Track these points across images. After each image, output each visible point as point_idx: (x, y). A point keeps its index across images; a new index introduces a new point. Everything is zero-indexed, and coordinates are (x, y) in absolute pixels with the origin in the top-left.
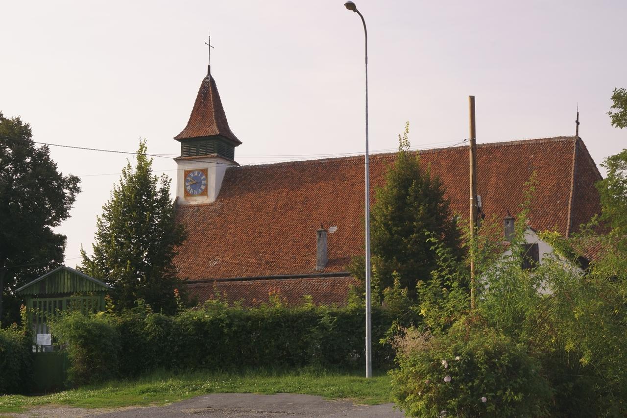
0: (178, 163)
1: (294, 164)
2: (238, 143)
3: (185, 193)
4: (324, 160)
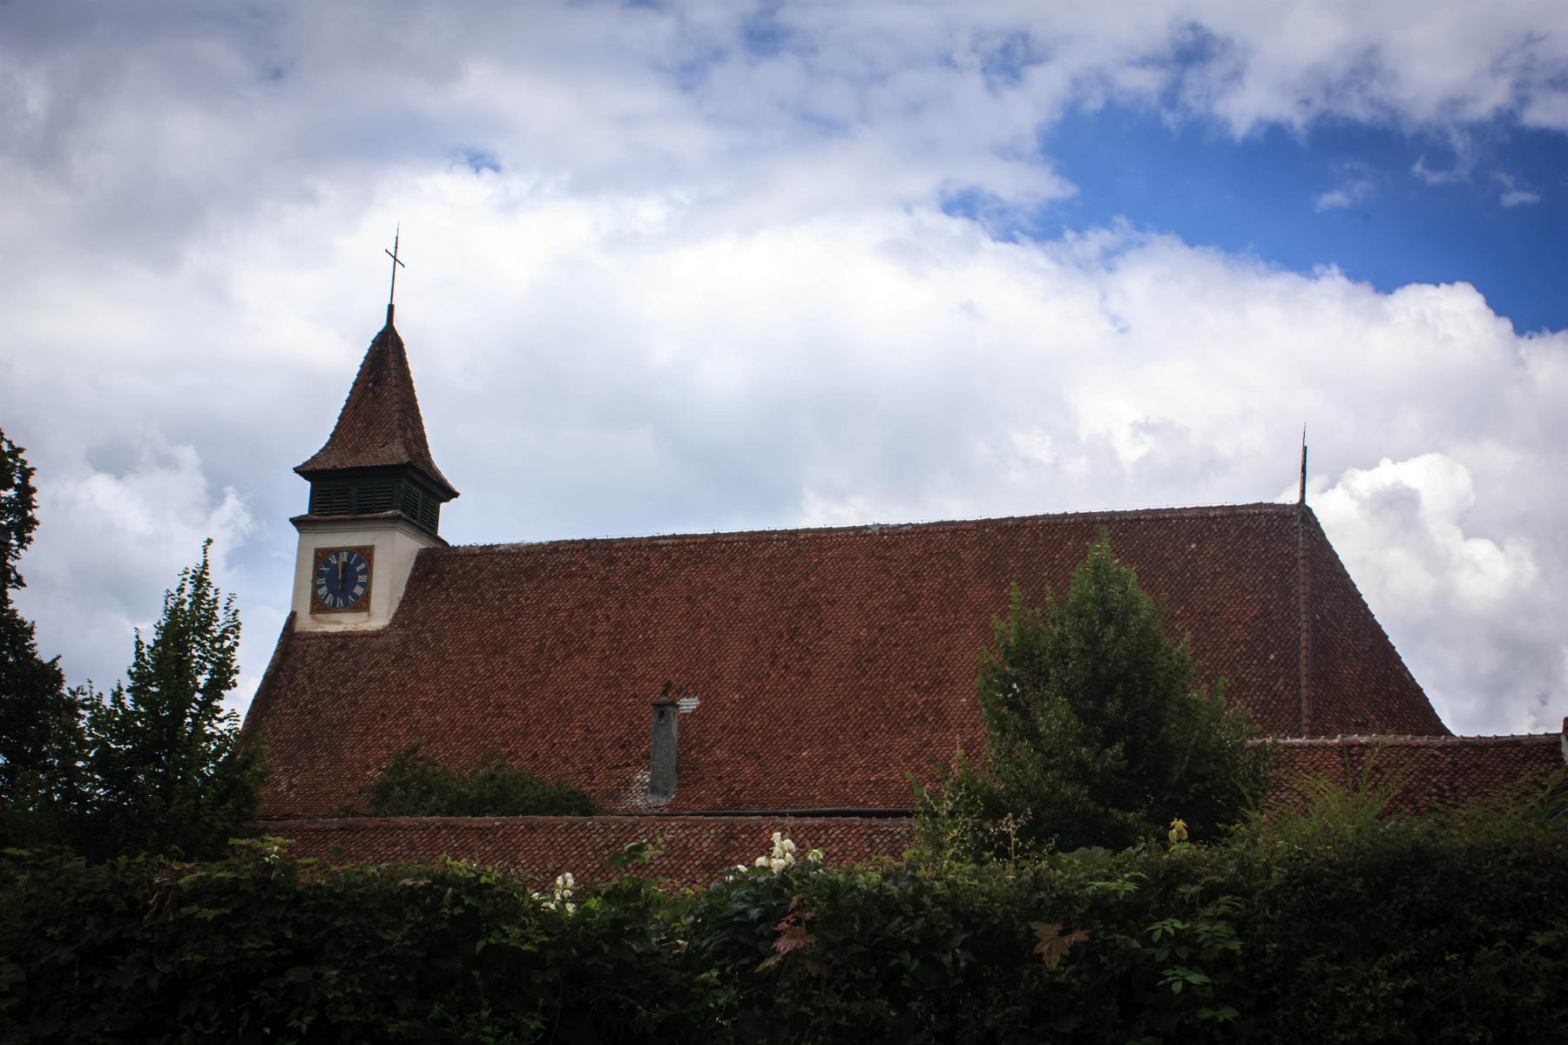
0: (299, 530)
1: (588, 546)
2: (451, 494)
4: (664, 538)
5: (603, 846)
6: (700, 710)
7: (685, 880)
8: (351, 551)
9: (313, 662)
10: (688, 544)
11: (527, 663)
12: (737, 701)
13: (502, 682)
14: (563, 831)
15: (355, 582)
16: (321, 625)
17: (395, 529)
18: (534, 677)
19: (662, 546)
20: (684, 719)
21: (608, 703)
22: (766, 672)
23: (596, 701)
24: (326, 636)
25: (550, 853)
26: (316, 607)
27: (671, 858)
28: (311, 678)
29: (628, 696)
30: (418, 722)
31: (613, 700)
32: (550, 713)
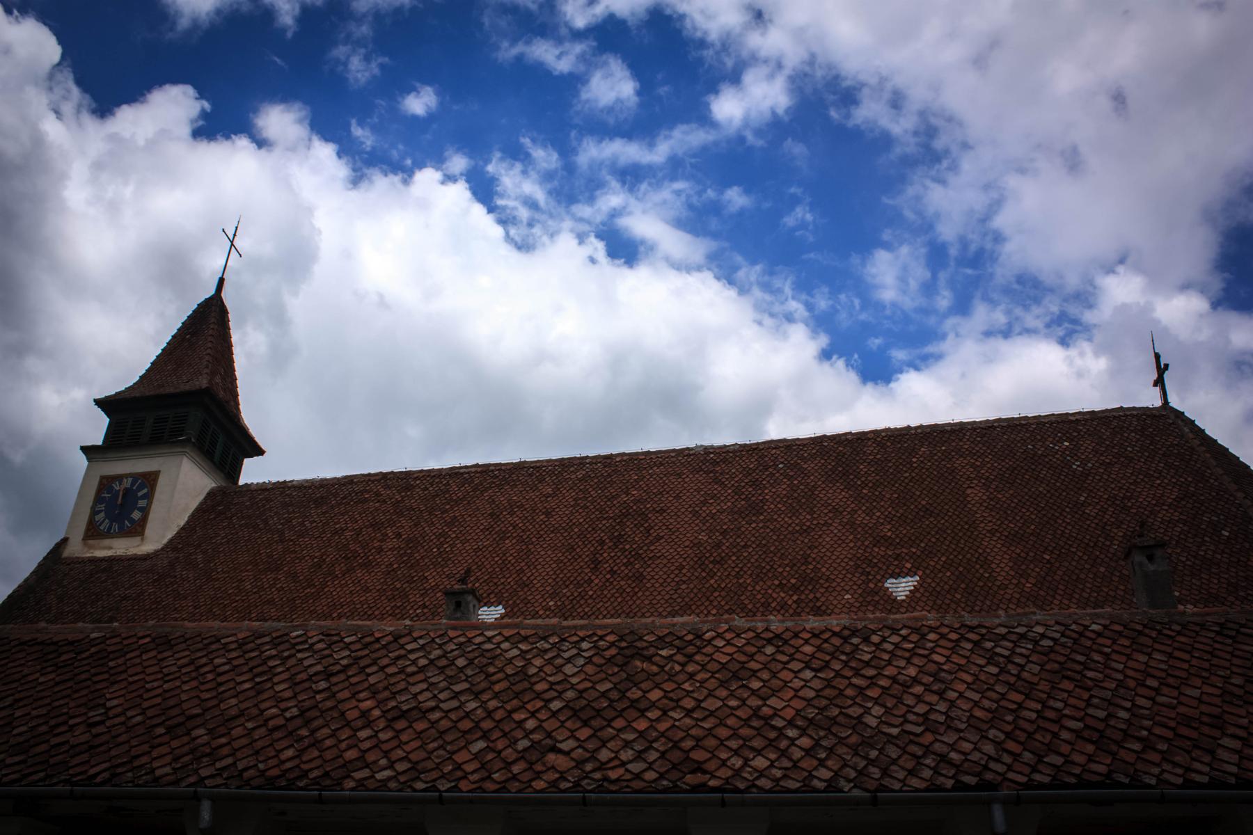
0: (88, 459)
1: (385, 479)
4: (466, 467)
5: (316, 674)
8: (135, 477)
10: (493, 471)
12: (553, 608)
13: (269, 597)
14: (233, 646)
15: (134, 507)
17: (184, 453)
18: (306, 592)
19: (462, 474)
21: (390, 615)
22: (586, 578)
23: (376, 613)
24: (94, 560)
25: (185, 687)
26: (90, 534)
27: (485, 697)
29: (415, 607)
31: (397, 611)
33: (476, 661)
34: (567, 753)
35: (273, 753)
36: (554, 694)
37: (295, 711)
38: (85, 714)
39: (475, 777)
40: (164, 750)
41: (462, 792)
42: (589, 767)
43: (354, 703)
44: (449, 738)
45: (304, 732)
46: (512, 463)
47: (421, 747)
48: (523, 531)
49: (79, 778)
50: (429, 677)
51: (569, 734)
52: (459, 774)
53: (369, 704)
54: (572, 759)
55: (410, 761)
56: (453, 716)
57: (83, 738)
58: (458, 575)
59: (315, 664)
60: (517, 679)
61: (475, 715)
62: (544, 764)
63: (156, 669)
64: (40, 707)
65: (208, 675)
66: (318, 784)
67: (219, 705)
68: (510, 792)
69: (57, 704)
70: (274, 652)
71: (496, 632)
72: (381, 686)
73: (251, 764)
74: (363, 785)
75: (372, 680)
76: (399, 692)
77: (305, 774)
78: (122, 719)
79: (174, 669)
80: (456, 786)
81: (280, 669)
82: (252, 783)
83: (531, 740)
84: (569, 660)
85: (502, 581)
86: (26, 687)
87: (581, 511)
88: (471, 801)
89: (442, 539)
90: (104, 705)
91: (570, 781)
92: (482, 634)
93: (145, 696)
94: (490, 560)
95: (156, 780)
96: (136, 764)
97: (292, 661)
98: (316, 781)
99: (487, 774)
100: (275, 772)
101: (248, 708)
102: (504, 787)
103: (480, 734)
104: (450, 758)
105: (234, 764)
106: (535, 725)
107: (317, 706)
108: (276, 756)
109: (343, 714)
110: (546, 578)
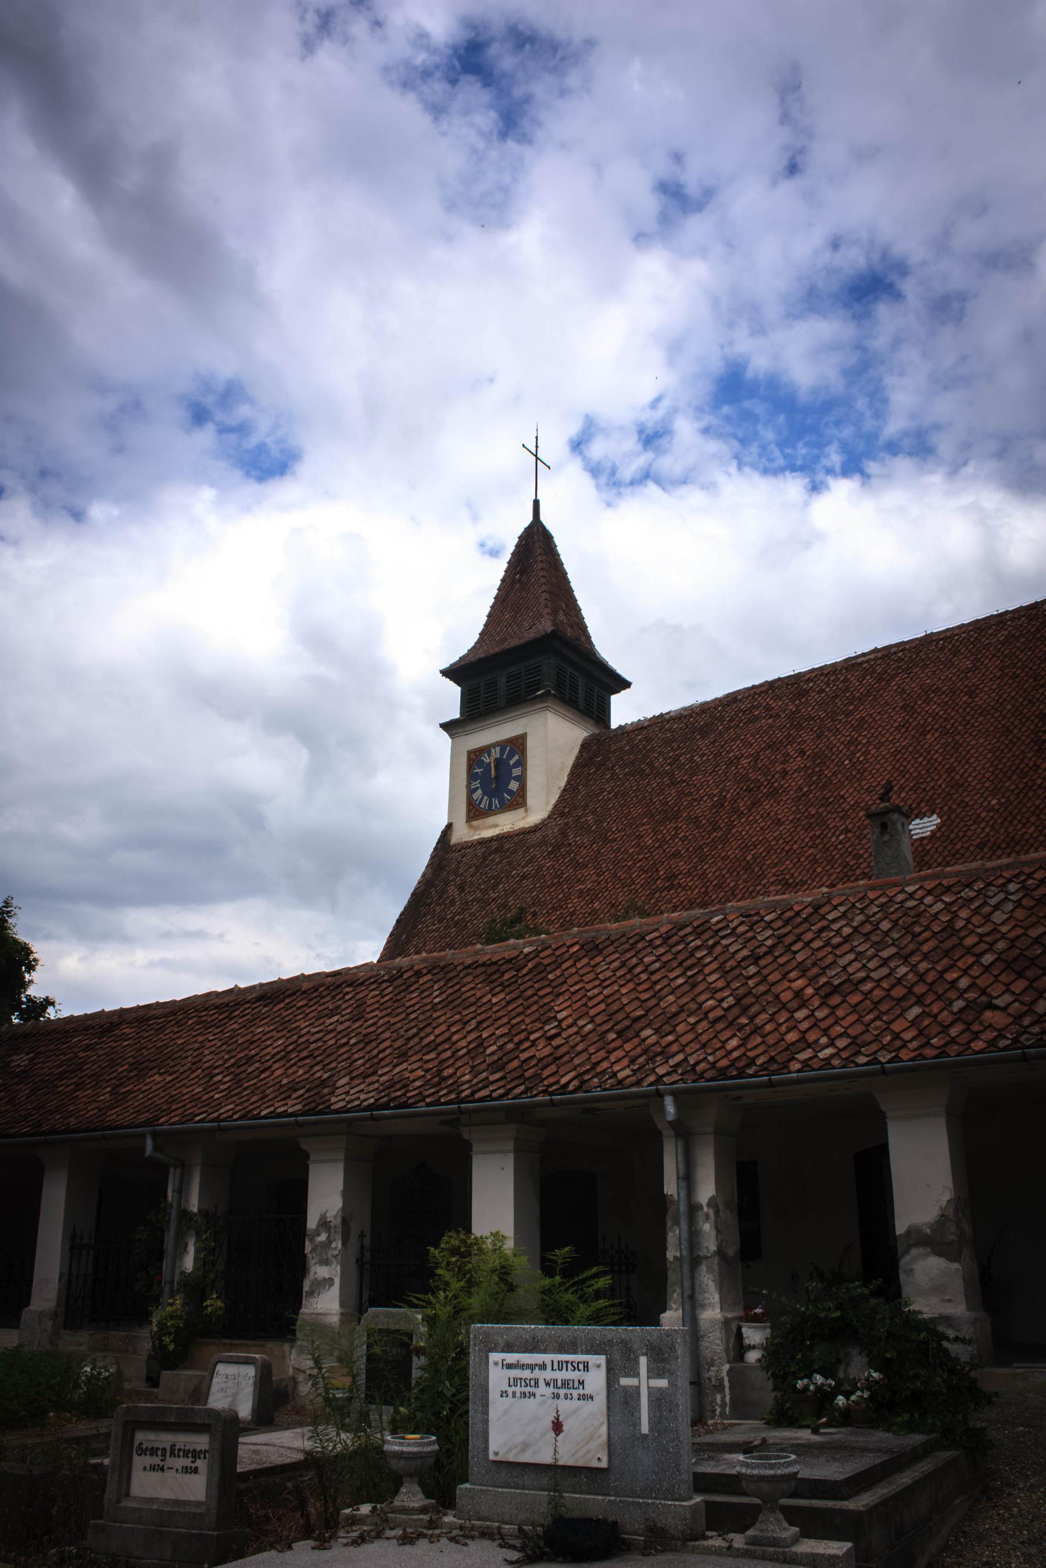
0: (450, 736)
1: (772, 688)
2: (623, 684)
3: (469, 811)
4: (864, 655)
5: (744, 959)
6: (943, 829)
7: (959, 1004)
8: (502, 744)
9: (466, 871)
10: (895, 653)
11: (704, 822)
12: (997, 807)
13: (673, 850)
14: (658, 942)
15: (510, 777)
16: (478, 833)
17: (546, 708)
18: (712, 837)
19: (861, 664)
20: (921, 845)
21: (811, 847)
22: (1031, 764)
23: (795, 847)
24: (483, 842)
25: (624, 991)
26: (472, 814)
27: (915, 959)
28: (461, 889)
29: (838, 833)
30: (573, 914)
31: (818, 842)
32: (735, 874)
33: (900, 922)
34: (1004, 1009)
35: (719, 1045)
36: (983, 947)
37: (731, 1000)
38: (542, 1028)
39: (914, 1044)
40: (619, 1053)
41: (903, 1061)
42: (1026, 1021)
43: (786, 984)
44: (884, 1007)
45: (744, 1020)
46: (917, 639)
47: (858, 1020)
48: (945, 720)
49: (554, 1087)
50: (856, 947)
51: (1004, 988)
52: (899, 1043)
53: (800, 983)
54: (1010, 1015)
55: (849, 1036)
56: (885, 985)
57: (548, 1050)
58: (880, 787)
59: (742, 949)
60: (945, 935)
61: (906, 980)
62: (981, 1023)
63: (591, 976)
64: (501, 1026)
65: (642, 975)
66: (766, 1069)
67: (657, 1004)
68: (949, 1056)
69: (514, 1021)
70: (698, 942)
71: (917, 887)
72: (809, 962)
73: (701, 1057)
74: (808, 1065)
75: (800, 957)
76: (828, 967)
77: (752, 1061)
78: (575, 1029)
79: (608, 974)
80: (896, 1056)
81: (708, 960)
82: (705, 1075)
83: (966, 1000)
84: (997, 907)
85: (932, 785)
86: (483, 1009)
87: (1010, 682)
88: (913, 1069)
89: (852, 748)
90: (555, 1017)
91: (1008, 1038)
92: (902, 891)
93: (590, 1004)
94: (912, 762)
95: (620, 1082)
96: (599, 1069)
97: (718, 949)
98: (763, 1067)
99: (925, 1040)
100: (724, 1063)
101: (686, 1004)
102: (944, 1052)
103: (913, 1000)
104: (888, 1028)
105: (685, 1060)
106: (967, 984)
107: (751, 992)
108: (723, 1047)
109: (777, 997)
110: (982, 772)
